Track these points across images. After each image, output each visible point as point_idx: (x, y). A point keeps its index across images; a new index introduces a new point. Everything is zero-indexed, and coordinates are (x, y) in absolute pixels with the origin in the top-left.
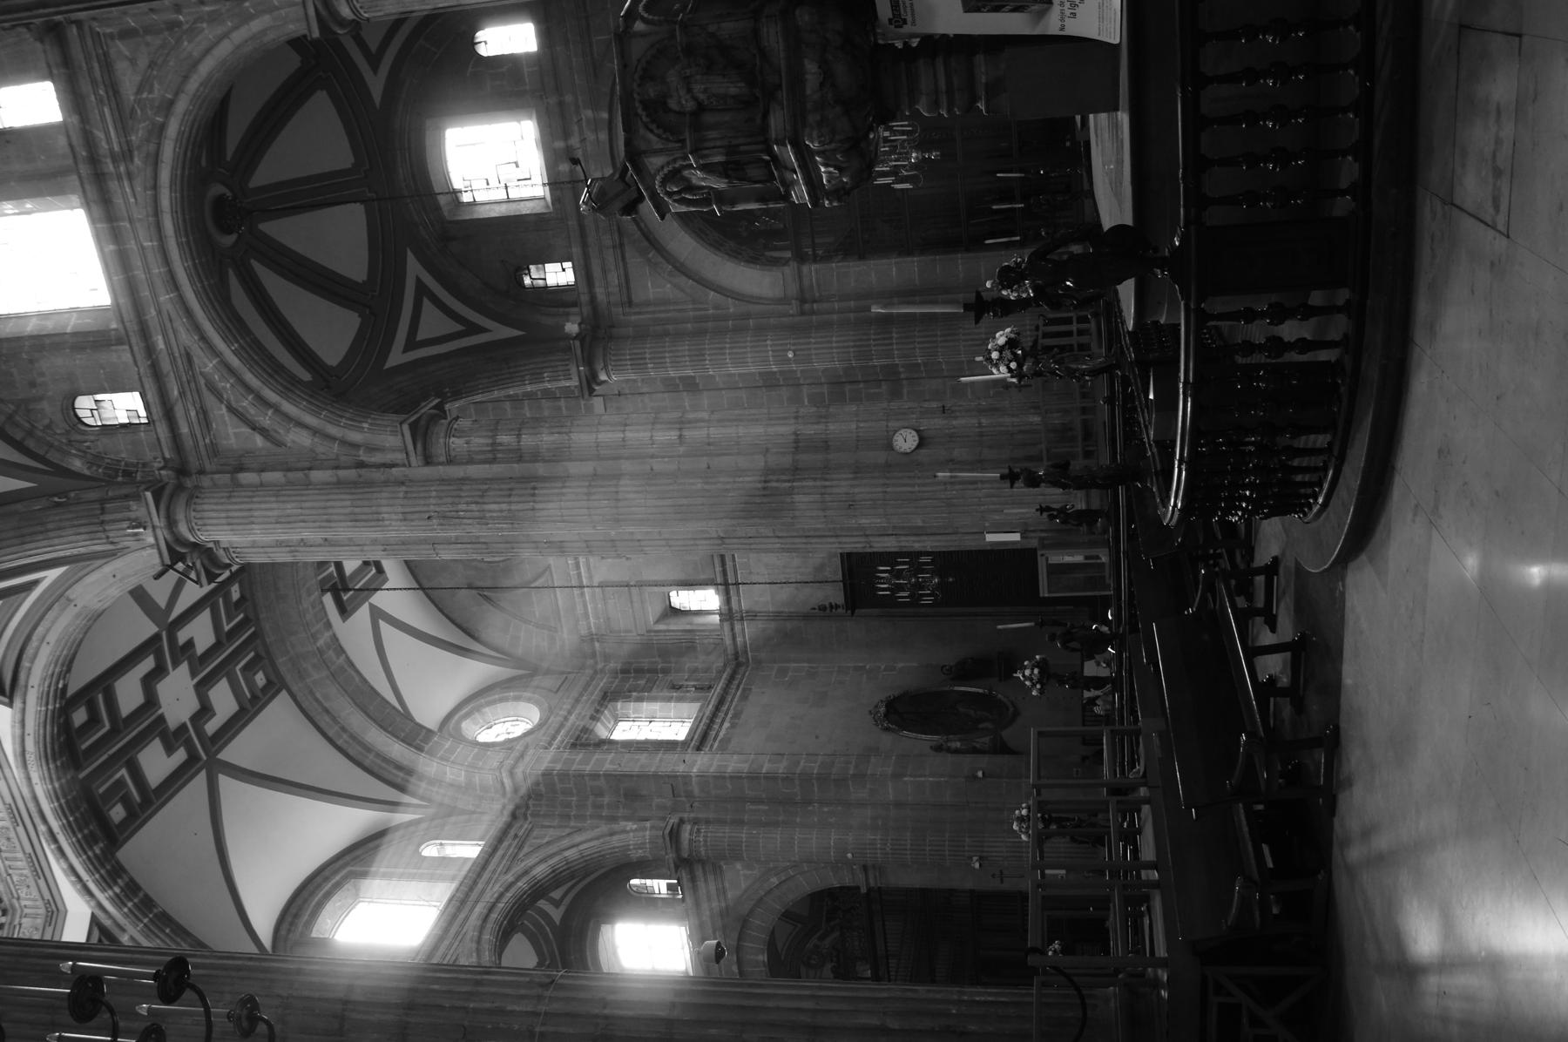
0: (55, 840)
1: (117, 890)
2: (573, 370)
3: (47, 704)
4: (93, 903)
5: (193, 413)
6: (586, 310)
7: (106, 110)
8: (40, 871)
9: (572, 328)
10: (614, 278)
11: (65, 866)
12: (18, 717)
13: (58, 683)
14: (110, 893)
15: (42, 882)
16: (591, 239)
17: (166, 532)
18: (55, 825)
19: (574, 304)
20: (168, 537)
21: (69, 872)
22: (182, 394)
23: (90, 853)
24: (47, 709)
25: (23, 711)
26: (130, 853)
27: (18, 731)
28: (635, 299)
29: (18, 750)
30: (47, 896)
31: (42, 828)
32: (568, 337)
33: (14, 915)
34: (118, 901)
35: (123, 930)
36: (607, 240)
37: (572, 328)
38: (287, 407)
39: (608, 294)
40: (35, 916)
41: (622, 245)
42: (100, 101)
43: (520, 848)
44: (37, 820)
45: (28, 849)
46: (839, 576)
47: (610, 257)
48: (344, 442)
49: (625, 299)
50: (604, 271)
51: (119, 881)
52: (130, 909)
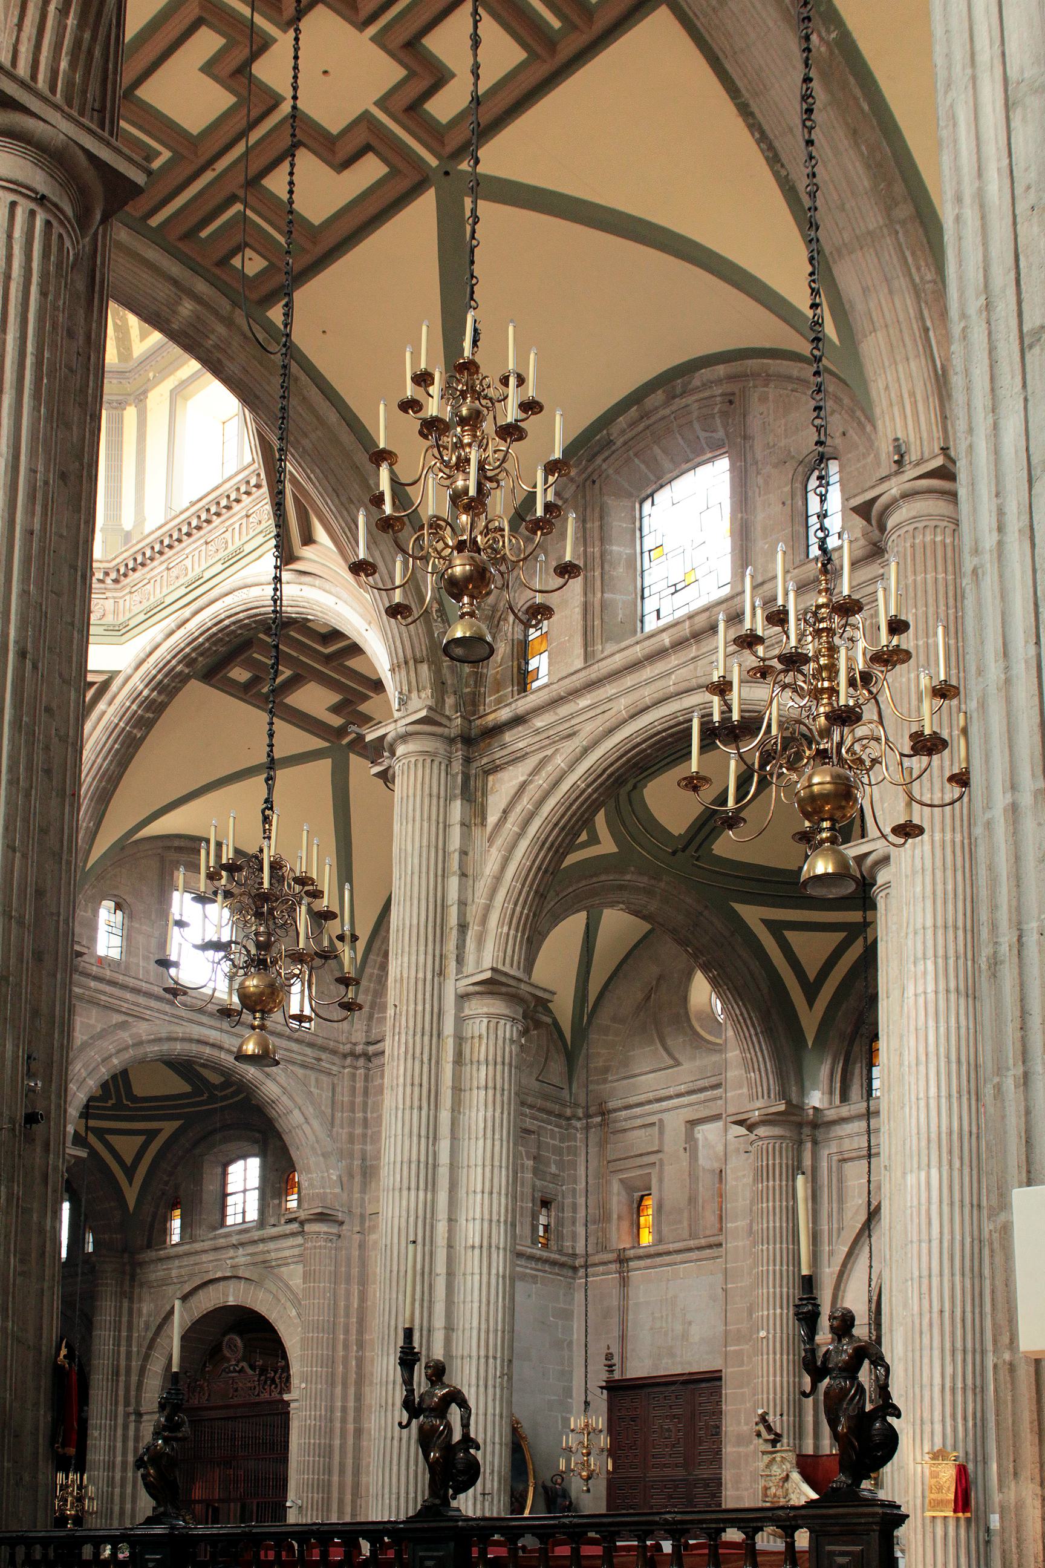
2: (759, 1104)
6: (831, 1114)
8: (151, 613)
9: (816, 1099)
11: (159, 639)
18: (191, 625)
19: (844, 1098)
21: (154, 644)
26: (196, 688)
29: (249, 581)
30: (132, 623)
31: (187, 612)
32: (802, 1092)
35: (110, 704)
37: (816, 1099)
38: (524, 844)
40: (115, 612)
43: (303, 1066)
45: (168, 601)
48: (488, 908)
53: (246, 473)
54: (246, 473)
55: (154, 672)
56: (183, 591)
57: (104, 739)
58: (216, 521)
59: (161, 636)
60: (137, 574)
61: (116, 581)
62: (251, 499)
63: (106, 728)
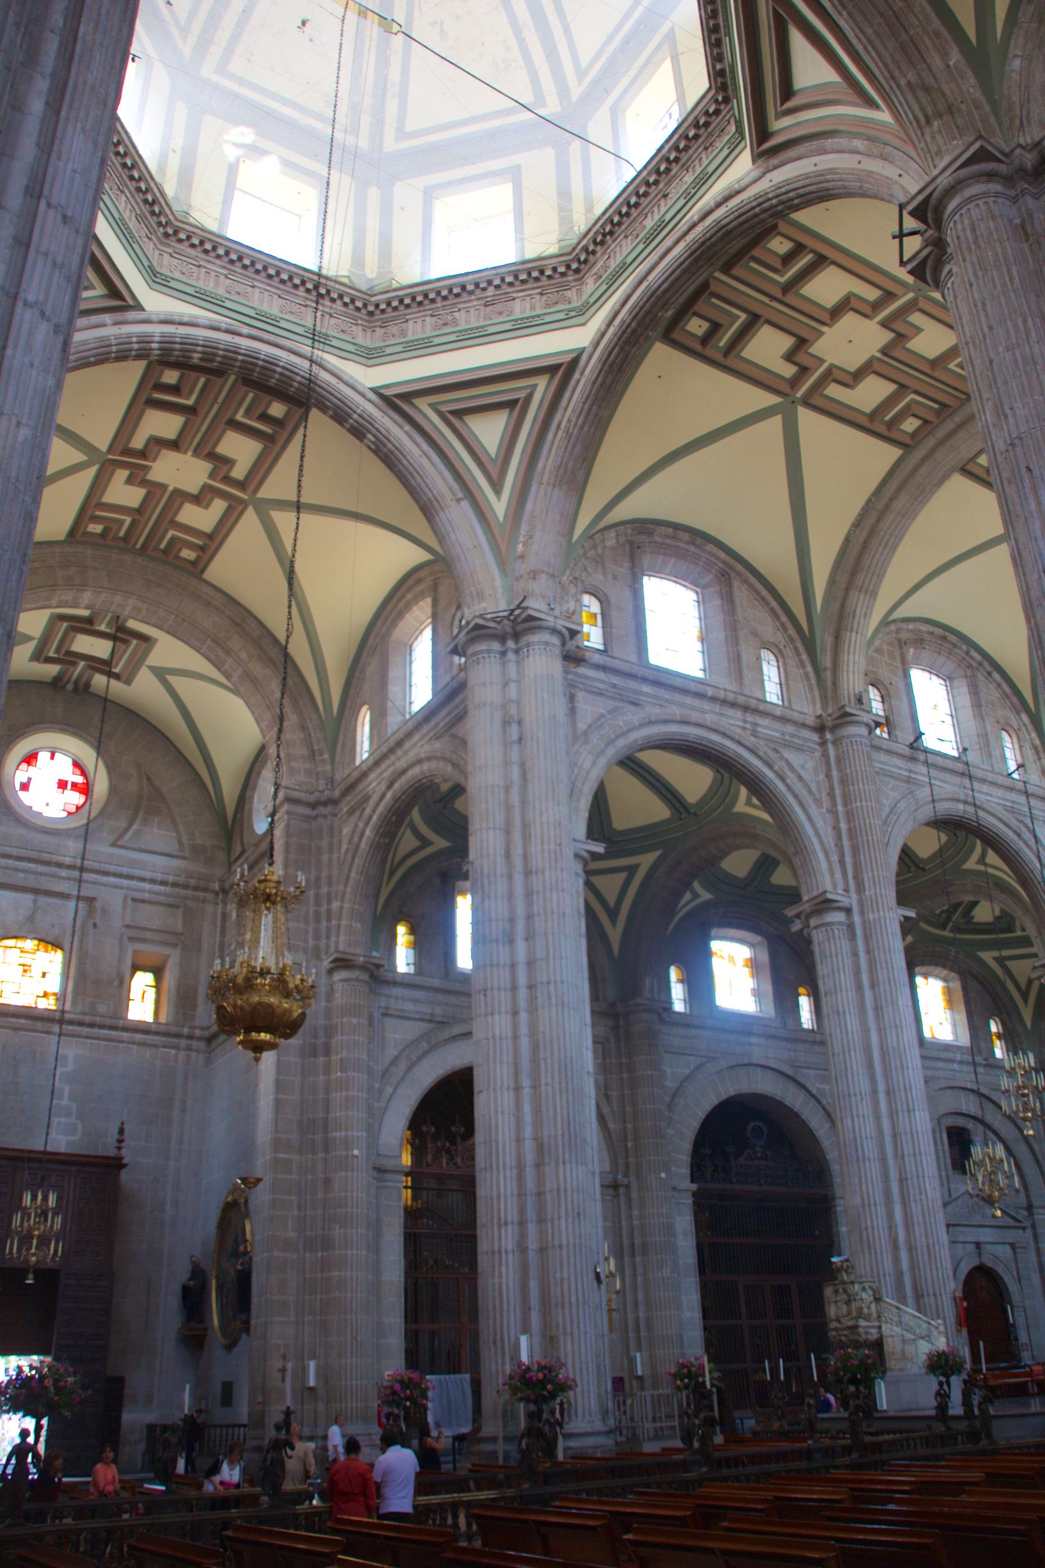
0: (227, 331)
1: (155, 346)
3: (360, 415)
4: (154, 318)
5: (600, 686)
7: (778, 735)
8: (201, 297)
10: (409, 1007)
11: (201, 321)
12: (360, 388)
13: (374, 436)
14: (157, 339)
15: (191, 291)
16: (440, 997)
17: (551, 624)
18: (245, 343)
20: (544, 624)
22: (615, 686)
23: (199, 349)
24: (355, 412)
25: (363, 396)
27: (346, 378)
28: (387, 1020)
30: (172, 284)
31: (245, 330)
33: (159, 240)
34: (145, 340)
35: (116, 323)
36: (438, 1011)
39: (397, 998)
41: (431, 1021)
42: (783, 734)
44: (254, 332)
46: (49, 1149)
47: (425, 1009)
49: (390, 1012)
50: (415, 1001)
51: (158, 352)
52: (132, 343)
53: (359, 294)
54: (359, 294)
55: (178, 340)
56: (252, 313)
57: (92, 346)
58: (301, 292)
59: (207, 323)
60: (192, 252)
61: (166, 235)
62: (342, 309)
63: (101, 339)
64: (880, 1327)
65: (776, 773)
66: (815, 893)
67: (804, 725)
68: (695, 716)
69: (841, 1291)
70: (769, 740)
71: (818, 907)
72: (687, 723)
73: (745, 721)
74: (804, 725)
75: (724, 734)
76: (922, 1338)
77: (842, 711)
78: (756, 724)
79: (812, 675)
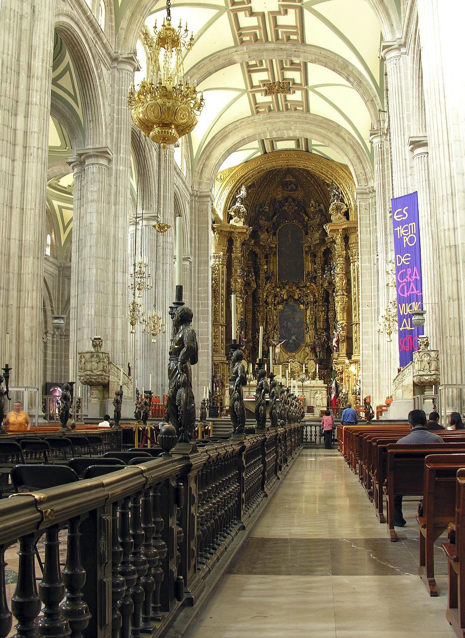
64: (109, 377)
65: (98, 73)
66: (97, 146)
67: (109, 54)
68: (81, 23)
69: (95, 356)
70: (98, 53)
71: (98, 154)
72: (78, 25)
73: (94, 38)
74: (109, 54)
75: (87, 40)
76: (125, 384)
77: (130, 56)
78: (96, 42)
79: (114, 28)
